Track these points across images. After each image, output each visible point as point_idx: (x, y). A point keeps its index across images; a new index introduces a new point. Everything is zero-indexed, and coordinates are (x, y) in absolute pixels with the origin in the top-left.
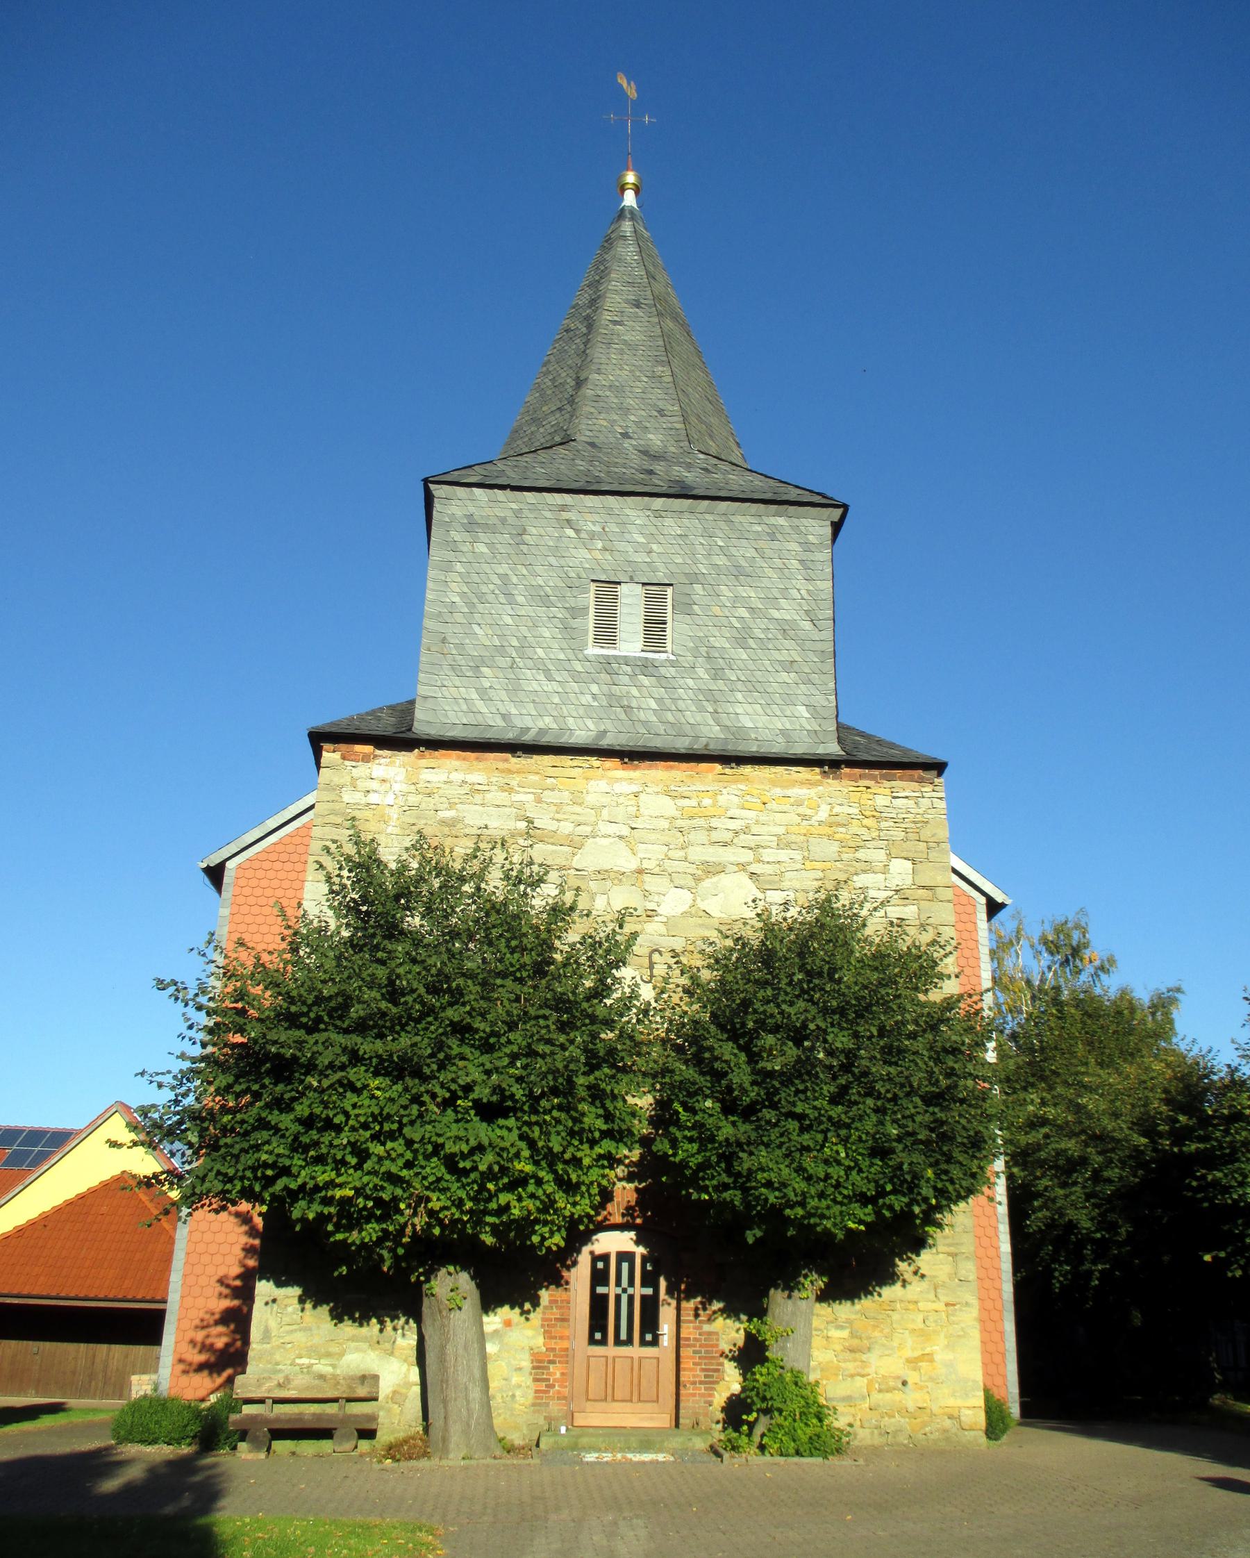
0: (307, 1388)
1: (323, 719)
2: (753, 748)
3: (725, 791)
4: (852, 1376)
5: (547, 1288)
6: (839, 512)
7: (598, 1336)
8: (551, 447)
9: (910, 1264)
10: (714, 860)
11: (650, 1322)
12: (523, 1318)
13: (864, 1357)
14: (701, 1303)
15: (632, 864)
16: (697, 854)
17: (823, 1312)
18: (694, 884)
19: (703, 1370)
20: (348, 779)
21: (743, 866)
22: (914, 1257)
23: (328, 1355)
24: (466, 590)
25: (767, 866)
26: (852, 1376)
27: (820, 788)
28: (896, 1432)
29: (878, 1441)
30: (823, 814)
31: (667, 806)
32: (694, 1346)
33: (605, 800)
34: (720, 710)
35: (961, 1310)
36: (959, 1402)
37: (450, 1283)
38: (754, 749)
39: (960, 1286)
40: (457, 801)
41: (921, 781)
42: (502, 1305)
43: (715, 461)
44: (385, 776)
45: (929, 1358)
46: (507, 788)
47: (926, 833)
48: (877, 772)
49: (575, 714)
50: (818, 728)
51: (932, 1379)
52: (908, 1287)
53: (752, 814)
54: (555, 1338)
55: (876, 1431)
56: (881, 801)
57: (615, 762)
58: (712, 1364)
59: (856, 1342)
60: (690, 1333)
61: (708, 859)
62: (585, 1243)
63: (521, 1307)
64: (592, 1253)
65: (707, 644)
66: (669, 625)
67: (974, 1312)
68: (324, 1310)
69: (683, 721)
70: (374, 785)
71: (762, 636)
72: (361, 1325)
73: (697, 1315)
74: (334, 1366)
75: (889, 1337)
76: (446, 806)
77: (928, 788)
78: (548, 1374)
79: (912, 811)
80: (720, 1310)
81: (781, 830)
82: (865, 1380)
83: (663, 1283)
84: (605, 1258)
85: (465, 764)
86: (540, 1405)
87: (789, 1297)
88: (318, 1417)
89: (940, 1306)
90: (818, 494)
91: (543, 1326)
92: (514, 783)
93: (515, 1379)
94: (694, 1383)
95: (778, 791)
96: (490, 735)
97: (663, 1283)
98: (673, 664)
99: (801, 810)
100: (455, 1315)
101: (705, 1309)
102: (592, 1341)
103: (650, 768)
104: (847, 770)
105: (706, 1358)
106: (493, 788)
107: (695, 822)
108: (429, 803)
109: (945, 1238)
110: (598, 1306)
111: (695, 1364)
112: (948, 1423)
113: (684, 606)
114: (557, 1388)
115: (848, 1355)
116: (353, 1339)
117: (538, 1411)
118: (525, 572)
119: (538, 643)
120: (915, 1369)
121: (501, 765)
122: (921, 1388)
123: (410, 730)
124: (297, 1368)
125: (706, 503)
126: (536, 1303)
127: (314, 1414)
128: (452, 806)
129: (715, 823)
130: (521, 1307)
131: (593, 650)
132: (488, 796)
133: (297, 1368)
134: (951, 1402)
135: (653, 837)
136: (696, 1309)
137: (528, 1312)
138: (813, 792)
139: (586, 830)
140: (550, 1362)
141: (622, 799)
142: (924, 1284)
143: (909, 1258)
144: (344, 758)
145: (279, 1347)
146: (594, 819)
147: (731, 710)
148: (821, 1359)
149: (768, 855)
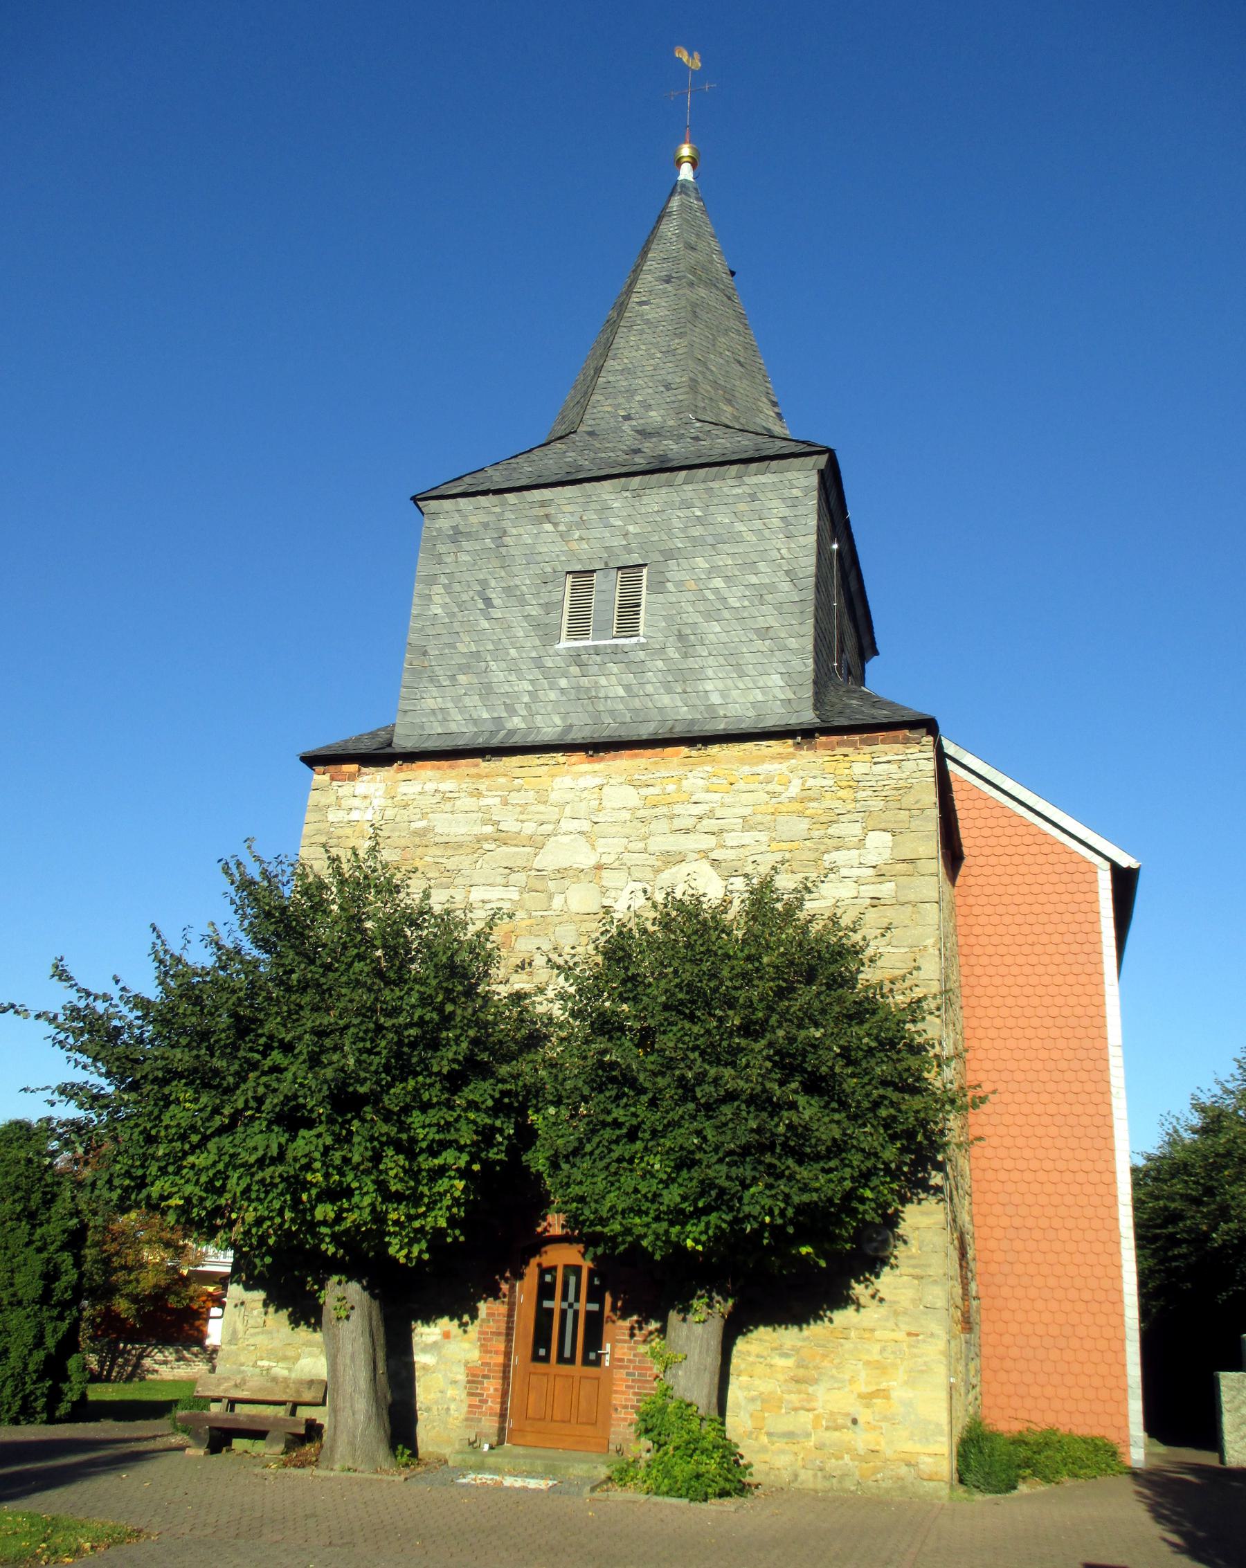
0: (260, 1390)
1: (314, 745)
2: (721, 727)
3: (689, 775)
4: (796, 1409)
5: (485, 1300)
6: (825, 458)
7: (542, 1352)
8: (548, 444)
9: (867, 1287)
10: (674, 849)
11: (594, 1339)
12: (461, 1331)
13: (811, 1389)
14: (637, 1322)
15: (592, 861)
16: (657, 844)
17: (766, 1338)
18: (652, 876)
19: (635, 1394)
20: (334, 798)
21: (704, 854)
22: (873, 1278)
23: (285, 1358)
24: (448, 600)
25: (730, 851)
26: (796, 1409)
27: (793, 761)
28: (844, 1476)
29: (821, 1484)
30: (794, 789)
31: (631, 796)
32: (627, 1367)
33: (569, 796)
34: (688, 690)
35: (924, 1341)
36: (918, 1448)
37: (339, 1291)
38: (722, 727)
39: (926, 1314)
40: (429, 810)
41: (906, 741)
42: (441, 1316)
43: (708, 427)
44: (368, 793)
45: (883, 1394)
46: (477, 793)
47: (908, 801)
48: (856, 737)
49: (543, 711)
50: (792, 696)
51: (885, 1419)
52: (862, 1310)
53: (716, 797)
54: (490, 1352)
55: (819, 1474)
56: (859, 769)
57: (579, 757)
58: (645, 1388)
59: (801, 1372)
60: (624, 1354)
61: (669, 849)
62: (534, 1255)
63: (460, 1318)
64: (539, 1265)
65: (679, 621)
66: (643, 608)
67: (941, 1344)
68: (284, 1314)
69: (650, 705)
70: (356, 802)
71: (738, 605)
72: (315, 1331)
73: (632, 1335)
74: (290, 1370)
75: (839, 1367)
76: (419, 816)
77: (915, 749)
78: (482, 1389)
79: (894, 776)
80: (657, 1330)
81: (746, 811)
82: (811, 1415)
83: (608, 1299)
84: (552, 1270)
85: (438, 774)
86: (472, 1420)
87: (684, 1320)
88: (251, 1418)
89: (900, 1335)
90: (803, 442)
91: (479, 1339)
92: (482, 787)
93: (450, 1392)
94: (626, 1407)
95: (747, 769)
96: (461, 742)
97: (608, 1299)
98: (643, 647)
99: (770, 788)
100: (344, 1324)
101: (641, 1329)
102: (536, 1358)
103: (615, 758)
104: (823, 739)
105: (639, 1381)
106: (462, 795)
107: (658, 811)
108: (404, 815)
109: (909, 1257)
110: (543, 1319)
111: (628, 1387)
112: (903, 1470)
113: (658, 586)
114: (490, 1403)
115: (793, 1386)
116: (308, 1344)
117: (470, 1427)
118: (503, 574)
119: (512, 643)
120: (867, 1406)
121: (473, 771)
122: (874, 1428)
123: (390, 745)
124: (258, 1370)
125: (683, 473)
126: (474, 1317)
127: (248, 1416)
128: (424, 815)
129: (677, 809)
130: (460, 1318)
131: (565, 644)
132: (458, 803)
133: (258, 1370)
134: (909, 1447)
135: (614, 830)
136: (632, 1328)
137: (466, 1324)
138: (784, 767)
139: (548, 828)
140: (485, 1377)
141: (585, 794)
142: (883, 1310)
143: (867, 1280)
144: (332, 779)
145: (244, 1349)
146: (557, 817)
147: (701, 688)
148: (762, 1389)
149: (731, 839)
